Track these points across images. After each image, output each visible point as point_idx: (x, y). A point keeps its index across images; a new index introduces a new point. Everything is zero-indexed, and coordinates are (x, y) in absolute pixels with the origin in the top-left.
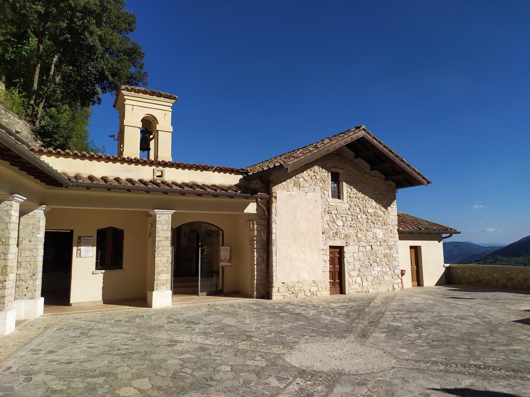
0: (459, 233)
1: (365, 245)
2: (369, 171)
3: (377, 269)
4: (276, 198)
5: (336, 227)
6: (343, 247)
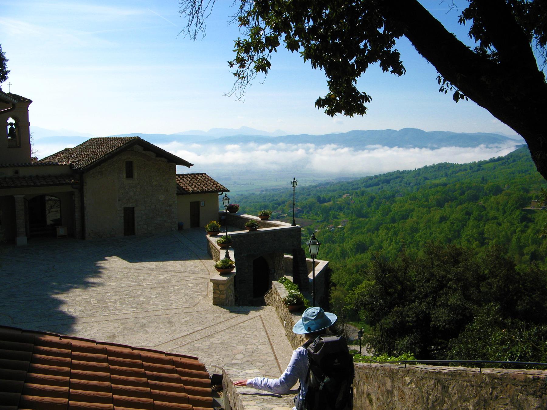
0: (229, 191)
4: (86, 183)
6: (134, 208)
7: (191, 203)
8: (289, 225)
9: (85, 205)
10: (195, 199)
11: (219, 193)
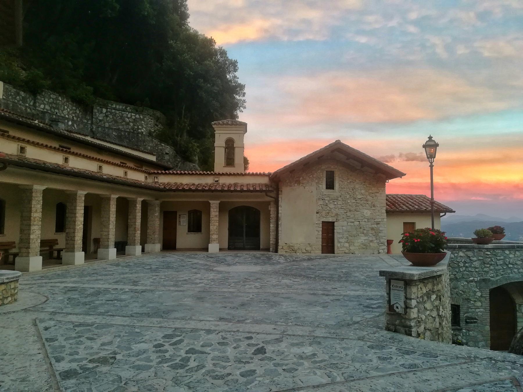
0: (454, 212)
1: (353, 221)
5: (328, 208)
11: (442, 214)
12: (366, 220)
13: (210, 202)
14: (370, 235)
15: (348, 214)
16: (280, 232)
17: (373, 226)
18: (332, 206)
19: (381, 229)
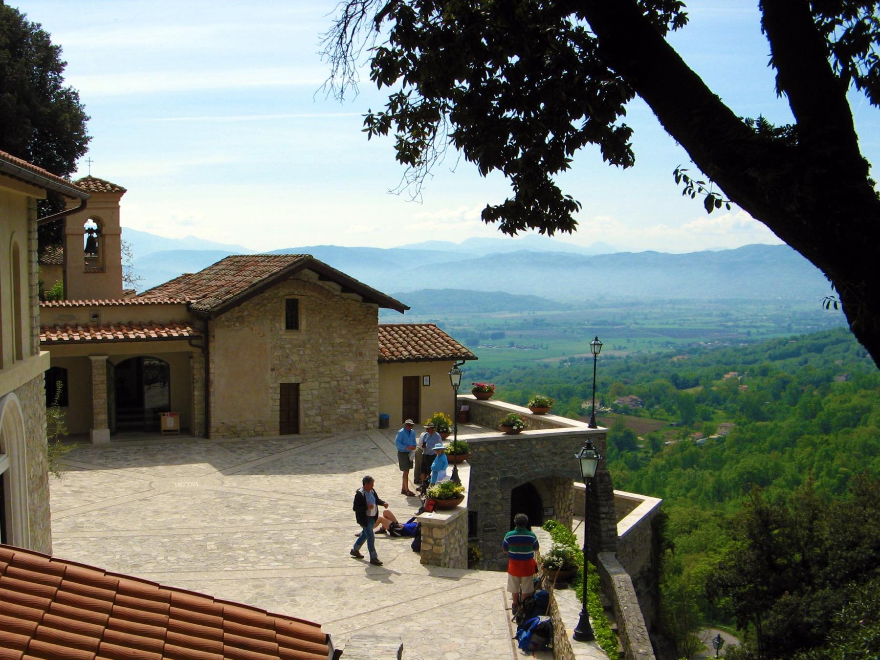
1: (329, 380)
2: (338, 293)
3: (343, 407)
4: (214, 337)
6: (298, 384)
7: (404, 378)
8: (582, 426)
9: (212, 377)
10: (412, 371)
12: (348, 378)
13: (93, 358)
14: (354, 401)
15: (321, 369)
16: (212, 405)
17: (359, 387)
18: (295, 358)
19: (370, 390)
